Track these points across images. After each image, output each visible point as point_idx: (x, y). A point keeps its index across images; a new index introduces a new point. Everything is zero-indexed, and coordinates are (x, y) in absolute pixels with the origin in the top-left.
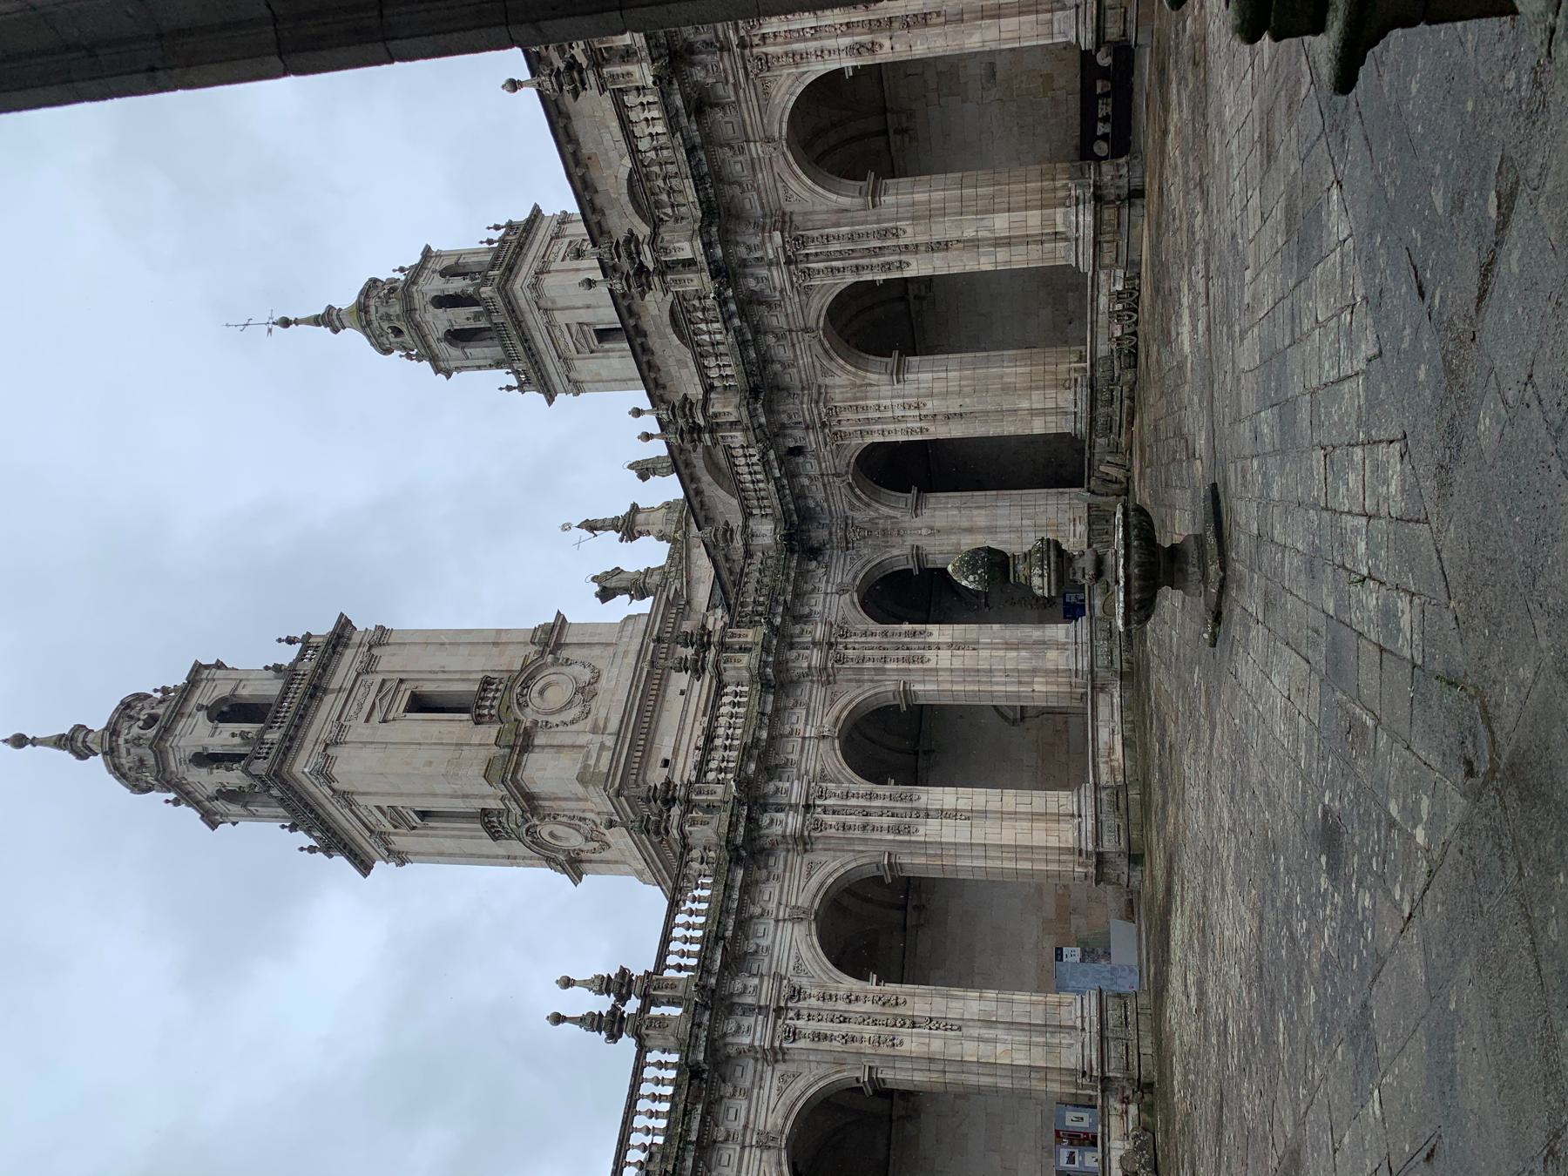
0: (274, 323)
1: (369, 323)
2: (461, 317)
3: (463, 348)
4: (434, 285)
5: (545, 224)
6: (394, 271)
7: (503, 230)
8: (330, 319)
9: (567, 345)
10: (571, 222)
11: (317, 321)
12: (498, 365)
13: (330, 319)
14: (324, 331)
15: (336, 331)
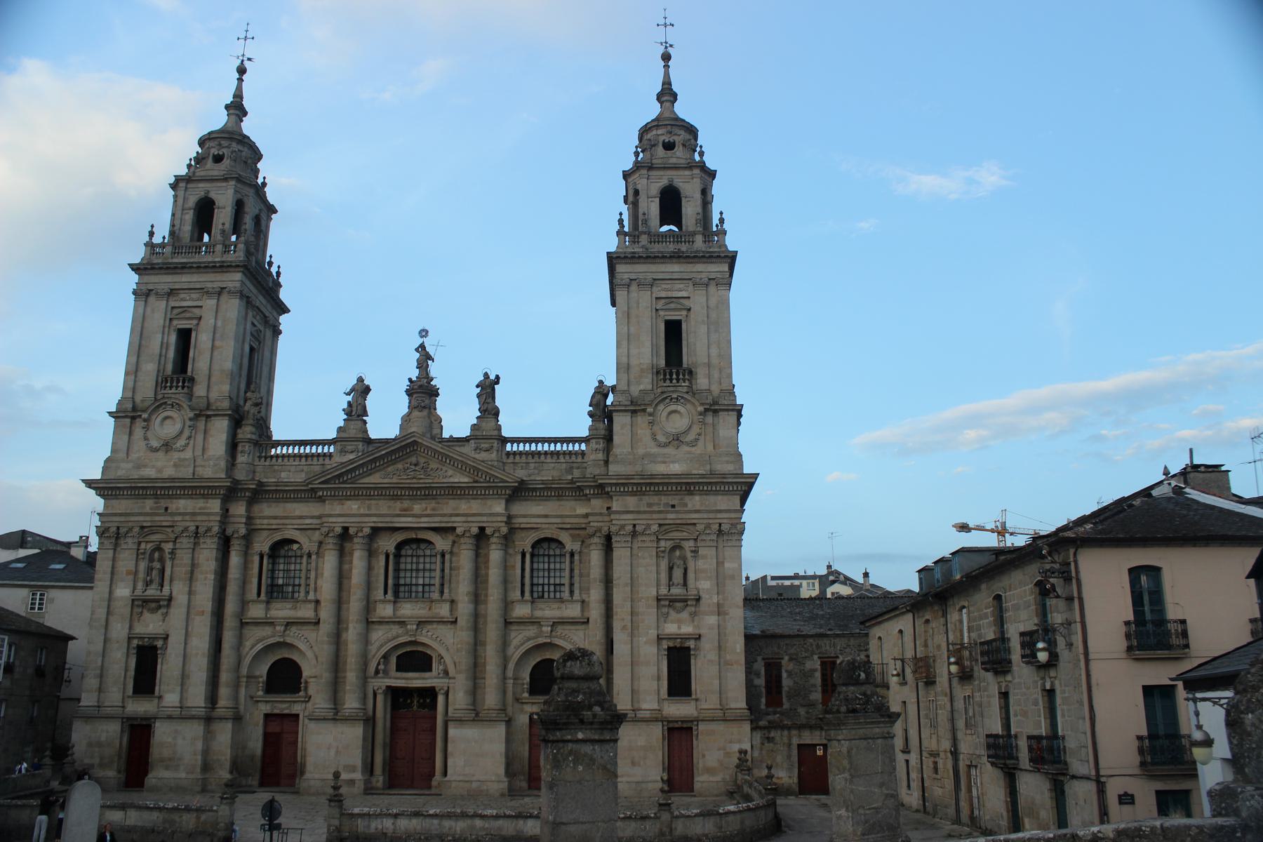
0: (243, 61)
1: (231, 139)
2: (223, 217)
3: (195, 210)
4: (251, 208)
5: (275, 314)
6: (264, 178)
7: (275, 274)
8: (237, 108)
9: (182, 300)
10: (273, 337)
11: (238, 95)
12: (172, 233)
13: (237, 108)
14: (229, 99)
15: (227, 107)
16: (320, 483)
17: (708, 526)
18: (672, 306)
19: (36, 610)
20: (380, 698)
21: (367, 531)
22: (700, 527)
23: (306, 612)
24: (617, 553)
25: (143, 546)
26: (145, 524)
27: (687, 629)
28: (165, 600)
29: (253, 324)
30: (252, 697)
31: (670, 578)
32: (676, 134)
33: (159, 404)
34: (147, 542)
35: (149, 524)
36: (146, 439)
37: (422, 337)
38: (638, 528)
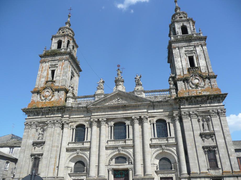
16: (91, 106)
17: (213, 111)
18: (189, 52)
19: (11, 153)
20: (110, 172)
21: (105, 119)
22: (210, 111)
23: (87, 145)
24: (184, 120)
25: (38, 127)
26: (39, 121)
27: (213, 144)
28: (42, 143)
29: (72, 70)
30: (69, 174)
31: (203, 128)
32: (182, 15)
33: (45, 88)
34: (39, 127)
35: (40, 121)
36: (40, 98)
37: (118, 67)
38: (190, 112)
